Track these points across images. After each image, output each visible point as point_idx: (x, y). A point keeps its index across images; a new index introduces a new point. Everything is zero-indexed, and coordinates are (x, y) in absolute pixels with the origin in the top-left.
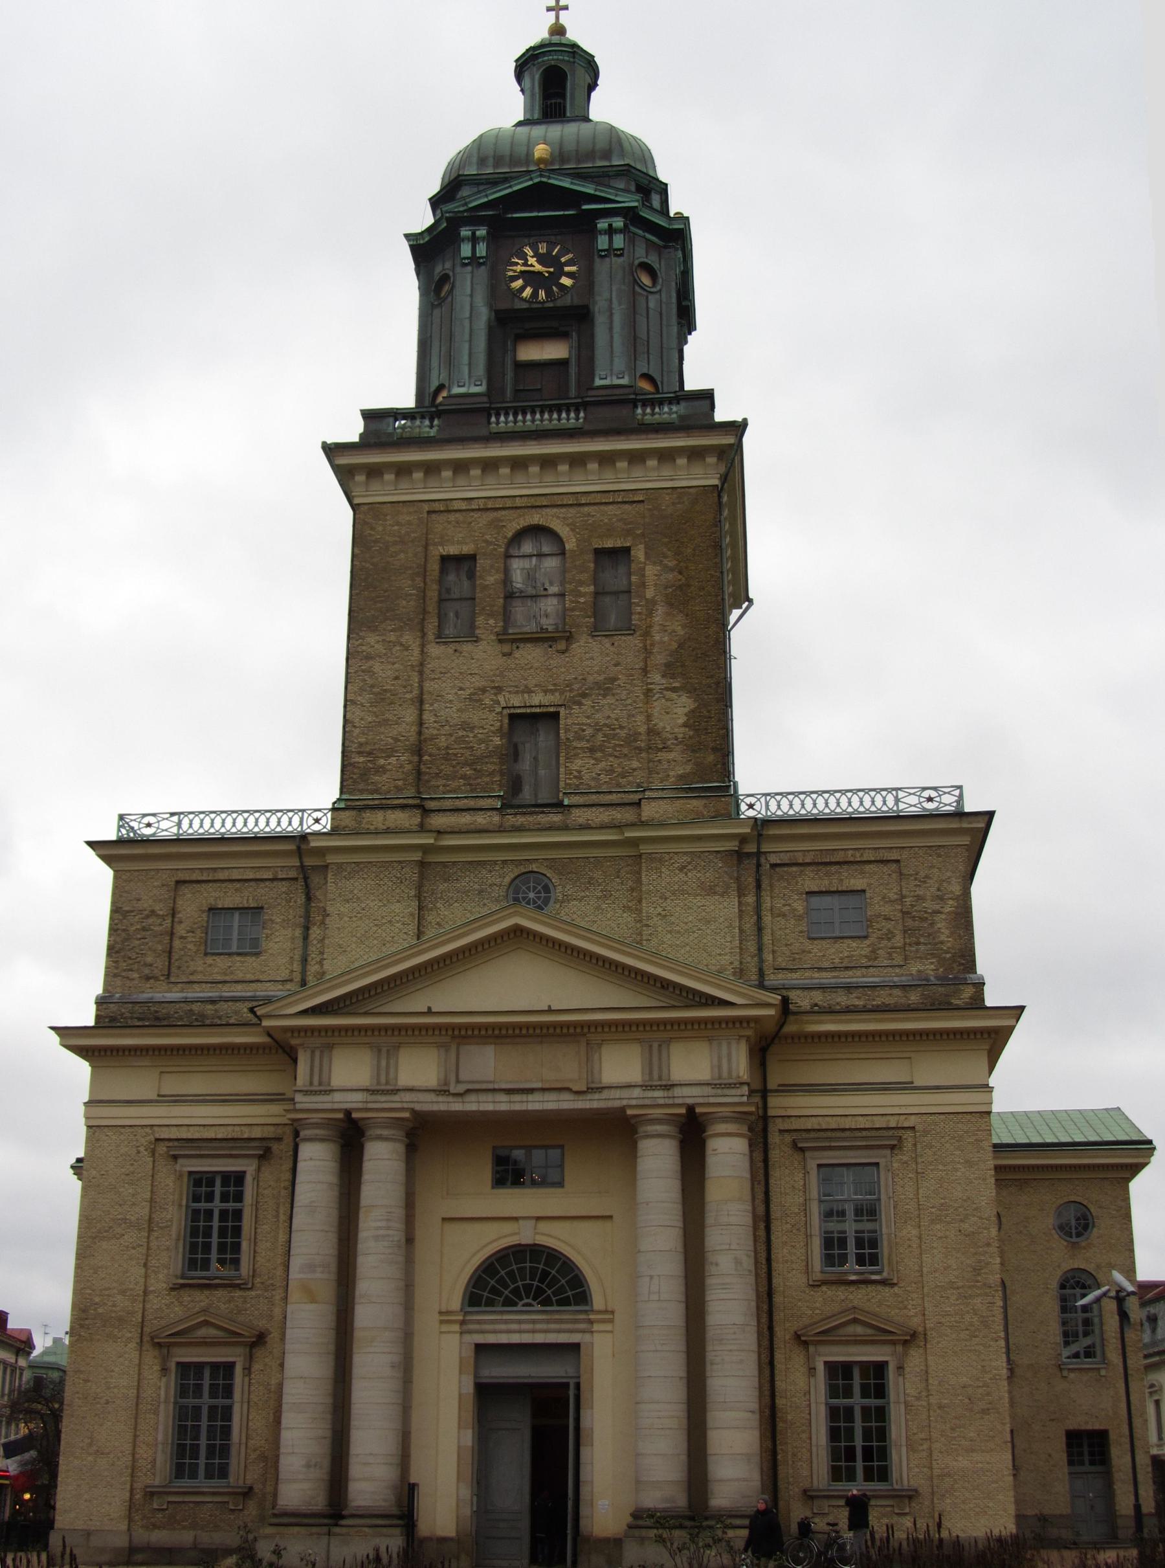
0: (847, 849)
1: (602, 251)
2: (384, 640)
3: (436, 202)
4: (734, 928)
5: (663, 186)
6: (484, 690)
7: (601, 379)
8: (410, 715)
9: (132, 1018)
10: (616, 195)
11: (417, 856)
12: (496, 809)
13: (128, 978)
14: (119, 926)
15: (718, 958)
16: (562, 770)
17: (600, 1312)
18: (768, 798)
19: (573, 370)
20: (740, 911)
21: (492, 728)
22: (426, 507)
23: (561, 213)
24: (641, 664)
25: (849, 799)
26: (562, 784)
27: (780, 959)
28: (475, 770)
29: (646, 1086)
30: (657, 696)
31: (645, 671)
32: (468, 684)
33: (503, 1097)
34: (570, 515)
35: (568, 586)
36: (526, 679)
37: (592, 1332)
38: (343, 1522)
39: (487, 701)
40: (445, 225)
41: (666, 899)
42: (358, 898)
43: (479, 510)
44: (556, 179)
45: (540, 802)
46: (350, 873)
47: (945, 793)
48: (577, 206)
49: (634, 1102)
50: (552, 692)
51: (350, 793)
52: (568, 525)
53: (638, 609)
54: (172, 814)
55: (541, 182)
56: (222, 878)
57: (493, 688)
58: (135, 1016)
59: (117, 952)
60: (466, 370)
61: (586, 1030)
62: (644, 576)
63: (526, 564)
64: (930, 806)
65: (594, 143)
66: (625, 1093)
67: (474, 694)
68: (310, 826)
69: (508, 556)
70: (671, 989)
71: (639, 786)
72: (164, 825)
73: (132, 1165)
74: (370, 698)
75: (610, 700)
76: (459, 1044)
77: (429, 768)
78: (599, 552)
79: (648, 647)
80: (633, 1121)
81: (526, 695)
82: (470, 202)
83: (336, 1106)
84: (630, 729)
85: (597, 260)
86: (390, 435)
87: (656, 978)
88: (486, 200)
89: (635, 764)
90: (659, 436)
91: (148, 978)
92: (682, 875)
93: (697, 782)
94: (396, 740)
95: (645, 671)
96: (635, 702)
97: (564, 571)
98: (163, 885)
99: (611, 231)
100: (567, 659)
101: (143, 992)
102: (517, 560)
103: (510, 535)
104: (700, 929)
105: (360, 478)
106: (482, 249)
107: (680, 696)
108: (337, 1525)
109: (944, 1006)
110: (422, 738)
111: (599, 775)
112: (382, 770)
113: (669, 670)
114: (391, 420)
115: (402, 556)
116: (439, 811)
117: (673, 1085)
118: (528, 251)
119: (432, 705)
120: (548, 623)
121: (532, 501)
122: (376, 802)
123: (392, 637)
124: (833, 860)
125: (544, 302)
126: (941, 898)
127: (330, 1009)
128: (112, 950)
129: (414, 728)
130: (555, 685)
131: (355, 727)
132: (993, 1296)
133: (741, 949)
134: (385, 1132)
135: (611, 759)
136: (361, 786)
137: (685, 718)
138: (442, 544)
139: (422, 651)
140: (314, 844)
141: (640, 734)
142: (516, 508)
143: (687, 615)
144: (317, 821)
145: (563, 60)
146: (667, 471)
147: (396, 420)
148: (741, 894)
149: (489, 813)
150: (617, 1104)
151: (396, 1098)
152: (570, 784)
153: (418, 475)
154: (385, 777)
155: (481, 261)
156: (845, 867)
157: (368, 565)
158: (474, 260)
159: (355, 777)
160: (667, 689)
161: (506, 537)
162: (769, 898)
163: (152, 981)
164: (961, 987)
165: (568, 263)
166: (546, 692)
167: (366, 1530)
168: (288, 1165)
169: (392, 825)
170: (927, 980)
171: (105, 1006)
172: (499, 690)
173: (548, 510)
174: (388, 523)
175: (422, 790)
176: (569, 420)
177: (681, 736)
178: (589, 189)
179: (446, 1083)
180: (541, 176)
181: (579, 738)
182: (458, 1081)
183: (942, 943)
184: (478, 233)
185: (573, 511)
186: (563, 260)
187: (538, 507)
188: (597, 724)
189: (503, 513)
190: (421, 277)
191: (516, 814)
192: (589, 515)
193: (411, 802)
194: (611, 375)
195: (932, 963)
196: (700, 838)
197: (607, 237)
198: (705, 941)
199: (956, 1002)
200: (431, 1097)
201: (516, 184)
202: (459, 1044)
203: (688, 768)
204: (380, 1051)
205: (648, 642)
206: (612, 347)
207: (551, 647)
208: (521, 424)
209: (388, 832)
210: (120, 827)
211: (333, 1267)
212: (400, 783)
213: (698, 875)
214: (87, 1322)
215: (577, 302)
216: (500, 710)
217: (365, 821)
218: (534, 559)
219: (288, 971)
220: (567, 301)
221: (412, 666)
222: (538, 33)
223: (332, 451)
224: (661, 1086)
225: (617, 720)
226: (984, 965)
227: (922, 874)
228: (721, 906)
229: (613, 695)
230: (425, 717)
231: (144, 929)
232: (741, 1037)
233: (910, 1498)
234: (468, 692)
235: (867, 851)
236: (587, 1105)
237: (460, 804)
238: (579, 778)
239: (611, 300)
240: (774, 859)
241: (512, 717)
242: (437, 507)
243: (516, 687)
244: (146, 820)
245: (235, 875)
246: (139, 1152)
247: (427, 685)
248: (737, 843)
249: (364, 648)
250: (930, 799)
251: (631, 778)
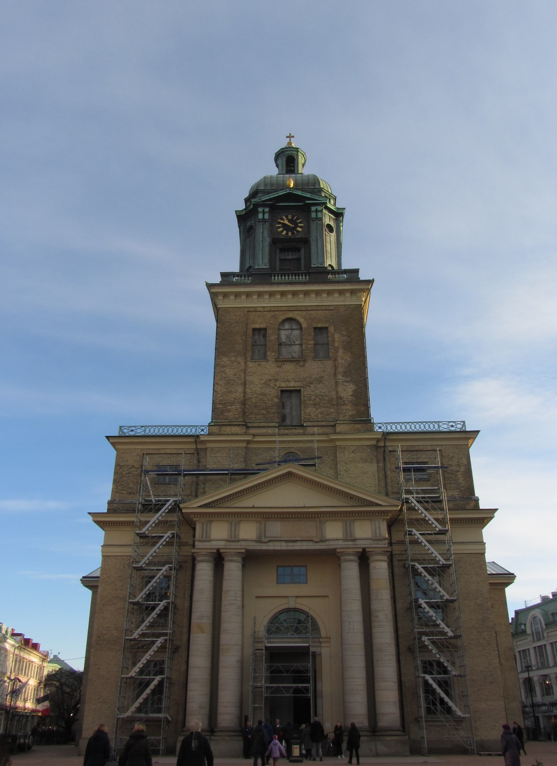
0: (420, 445)
1: (313, 218)
2: (230, 360)
3: (247, 200)
4: (375, 476)
5: (335, 198)
6: (270, 380)
7: (314, 265)
8: (240, 389)
9: (123, 510)
10: (319, 198)
11: (244, 445)
12: (276, 427)
13: (121, 493)
14: (119, 472)
15: (370, 488)
16: (302, 412)
17: (324, 638)
18: (387, 424)
19: (303, 262)
20: (378, 469)
21: (274, 395)
22: (247, 310)
23: (297, 204)
24: (333, 372)
25: (420, 426)
26: (302, 418)
27: (394, 489)
28: (267, 411)
29: (345, 540)
30: (341, 384)
31: (335, 374)
32: (264, 378)
33: (284, 544)
34: (304, 314)
35: (303, 341)
36: (287, 376)
37: (321, 647)
38: (215, 734)
39: (272, 385)
40: (252, 207)
41: (347, 464)
42: (220, 462)
43: (268, 311)
44: (295, 191)
45: (293, 425)
46: (216, 451)
47: (458, 424)
48: (304, 201)
49: (340, 546)
50: (298, 381)
51: (216, 420)
52: (303, 318)
53: (332, 350)
54: (142, 427)
55: (290, 192)
56: (162, 452)
57: (275, 379)
58: (125, 509)
59: (118, 482)
60: (261, 260)
61: (319, 515)
62: (334, 338)
63: (287, 332)
64: (452, 429)
65: (308, 181)
66: (336, 543)
67: (266, 382)
68: (199, 432)
69: (279, 329)
70: (354, 499)
71: (334, 419)
72: (139, 431)
73: (122, 573)
74: (224, 382)
75: (321, 385)
76: (265, 521)
77: (248, 410)
78: (315, 328)
79: (336, 365)
80: (339, 555)
81: (287, 383)
82: (262, 199)
83: (213, 547)
84: (330, 397)
85: (311, 222)
87: (348, 494)
88: (268, 198)
89: (332, 410)
90: (340, 285)
91: (130, 493)
92: (353, 455)
93: (358, 418)
94: (235, 399)
95: (335, 374)
96: (331, 386)
97: (302, 335)
98: (138, 455)
99: (317, 211)
100: (304, 369)
101: (128, 499)
102: (283, 331)
103: (280, 321)
104: (361, 476)
105: (221, 298)
106: (267, 216)
107: (349, 384)
108: (212, 735)
109: (463, 509)
110: (246, 398)
111: (318, 414)
112: (229, 411)
113: (345, 374)
114: (232, 277)
115: (237, 328)
116: (253, 427)
117: (356, 539)
118: (284, 217)
119: (249, 386)
120: (296, 355)
121: (289, 309)
122: (227, 423)
123: (233, 359)
124: (414, 450)
125: (291, 236)
126: (459, 465)
127: (211, 506)
128: (115, 481)
129: (242, 394)
130: (299, 379)
131: (218, 393)
132: (492, 632)
133: (379, 485)
134: (234, 558)
135: (322, 408)
136: (221, 417)
137: (352, 393)
138: (253, 324)
139: (245, 365)
140: (202, 438)
141: (334, 399)
142: (283, 311)
143: (351, 353)
144: (202, 430)
146: (341, 299)
147: (234, 277)
148: (378, 463)
149: (273, 429)
150: (332, 547)
151: (239, 544)
152: (306, 418)
153: (244, 297)
154: (230, 413)
155: (266, 220)
156: (419, 452)
157: (223, 331)
158: (264, 220)
159: (218, 413)
160: (344, 381)
161: (279, 322)
162: (389, 465)
163: (132, 495)
164: (470, 501)
165: (301, 223)
166: (296, 381)
167: (227, 738)
168: (189, 573)
169: (234, 433)
170: (456, 498)
171: (112, 505)
172: (276, 380)
173: (294, 312)
174: (232, 315)
175: (245, 419)
176: (302, 278)
177: (350, 400)
178: (308, 195)
179: (260, 537)
180: (290, 190)
181: (310, 400)
182: (265, 537)
183: (460, 483)
184: (265, 210)
185: (305, 313)
186: (298, 221)
187: (291, 311)
188: (316, 394)
189: (277, 312)
190: (242, 227)
191: (284, 429)
192: (312, 314)
193: (241, 423)
194: (318, 264)
195: (457, 492)
196: (360, 439)
197: (315, 213)
198: (364, 481)
199: (469, 508)
200: (253, 543)
201: (280, 193)
202: (265, 521)
203: (354, 412)
204: (231, 524)
205: (336, 363)
206: (318, 253)
207: (297, 364)
208: (284, 280)
209: (232, 434)
210: (120, 431)
211: (211, 618)
212: (237, 416)
213: (360, 454)
214: (100, 642)
215: (303, 237)
216: (277, 388)
217: (222, 431)
218: (290, 331)
219: (190, 491)
220: (300, 236)
221: (241, 370)
222: (284, 145)
223: (210, 286)
224: (351, 540)
225: (324, 393)
226: (478, 493)
227: (451, 456)
228: (370, 467)
229: (323, 383)
230: (246, 390)
231: (129, 473)
232: (384, 519)
233: (462, 721)
234: (264, 381)
235: (428, 446)
236: (320, 548)
237: (261, 425)
238: (310, 415)
239: (317, 237)
240: (390, 449)
241: (282, 391)
242: (250, 309)
243: (283, 379)
244: (131, 429)
245: (168, 452)
246: (125, 567)
247: (248, 378)
248: (375, 442)
249: (222, 363)
250: (452, 426)
251: (331, 416)
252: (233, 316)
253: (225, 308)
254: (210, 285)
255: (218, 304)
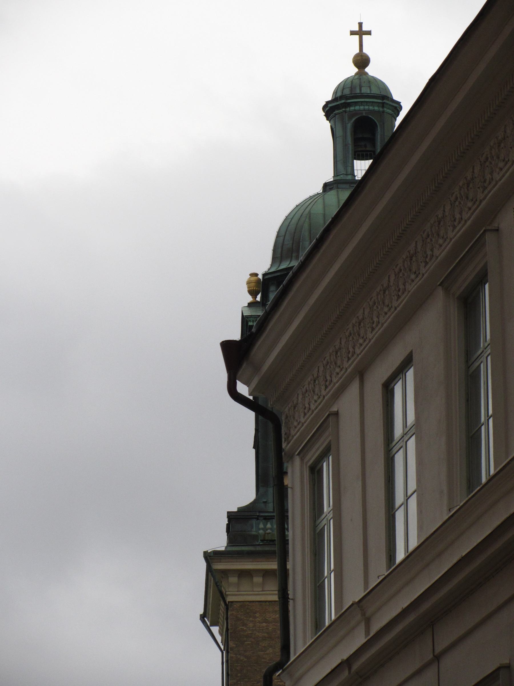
86: (256, 537)
105: (233, 580)
114: (254, 522)
145: (373, 112)
157: (242, 658)
174: (258, 620)
252: (262, 623)
253: (243, 604)
254: (212, 555)
255: (227, 593)
